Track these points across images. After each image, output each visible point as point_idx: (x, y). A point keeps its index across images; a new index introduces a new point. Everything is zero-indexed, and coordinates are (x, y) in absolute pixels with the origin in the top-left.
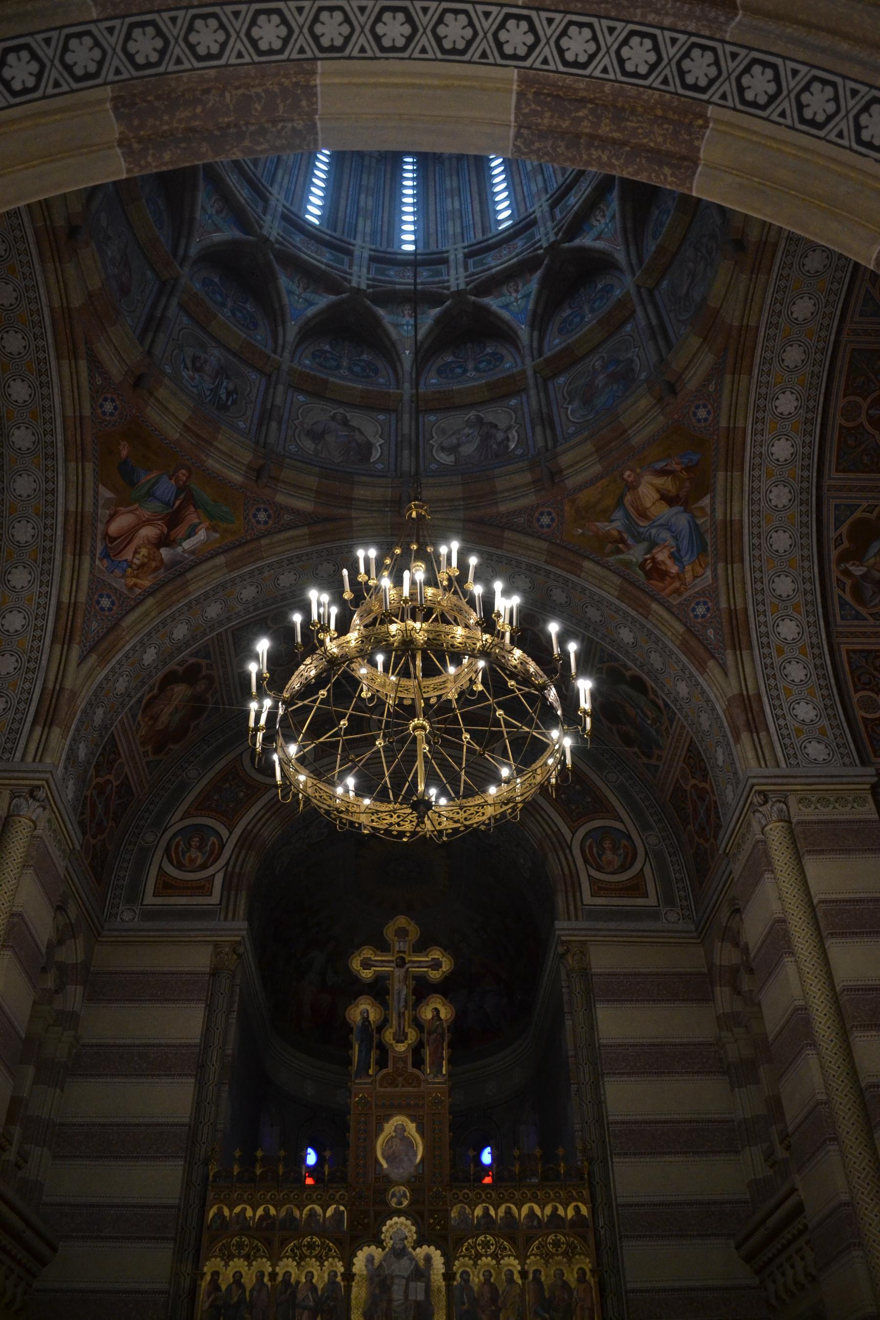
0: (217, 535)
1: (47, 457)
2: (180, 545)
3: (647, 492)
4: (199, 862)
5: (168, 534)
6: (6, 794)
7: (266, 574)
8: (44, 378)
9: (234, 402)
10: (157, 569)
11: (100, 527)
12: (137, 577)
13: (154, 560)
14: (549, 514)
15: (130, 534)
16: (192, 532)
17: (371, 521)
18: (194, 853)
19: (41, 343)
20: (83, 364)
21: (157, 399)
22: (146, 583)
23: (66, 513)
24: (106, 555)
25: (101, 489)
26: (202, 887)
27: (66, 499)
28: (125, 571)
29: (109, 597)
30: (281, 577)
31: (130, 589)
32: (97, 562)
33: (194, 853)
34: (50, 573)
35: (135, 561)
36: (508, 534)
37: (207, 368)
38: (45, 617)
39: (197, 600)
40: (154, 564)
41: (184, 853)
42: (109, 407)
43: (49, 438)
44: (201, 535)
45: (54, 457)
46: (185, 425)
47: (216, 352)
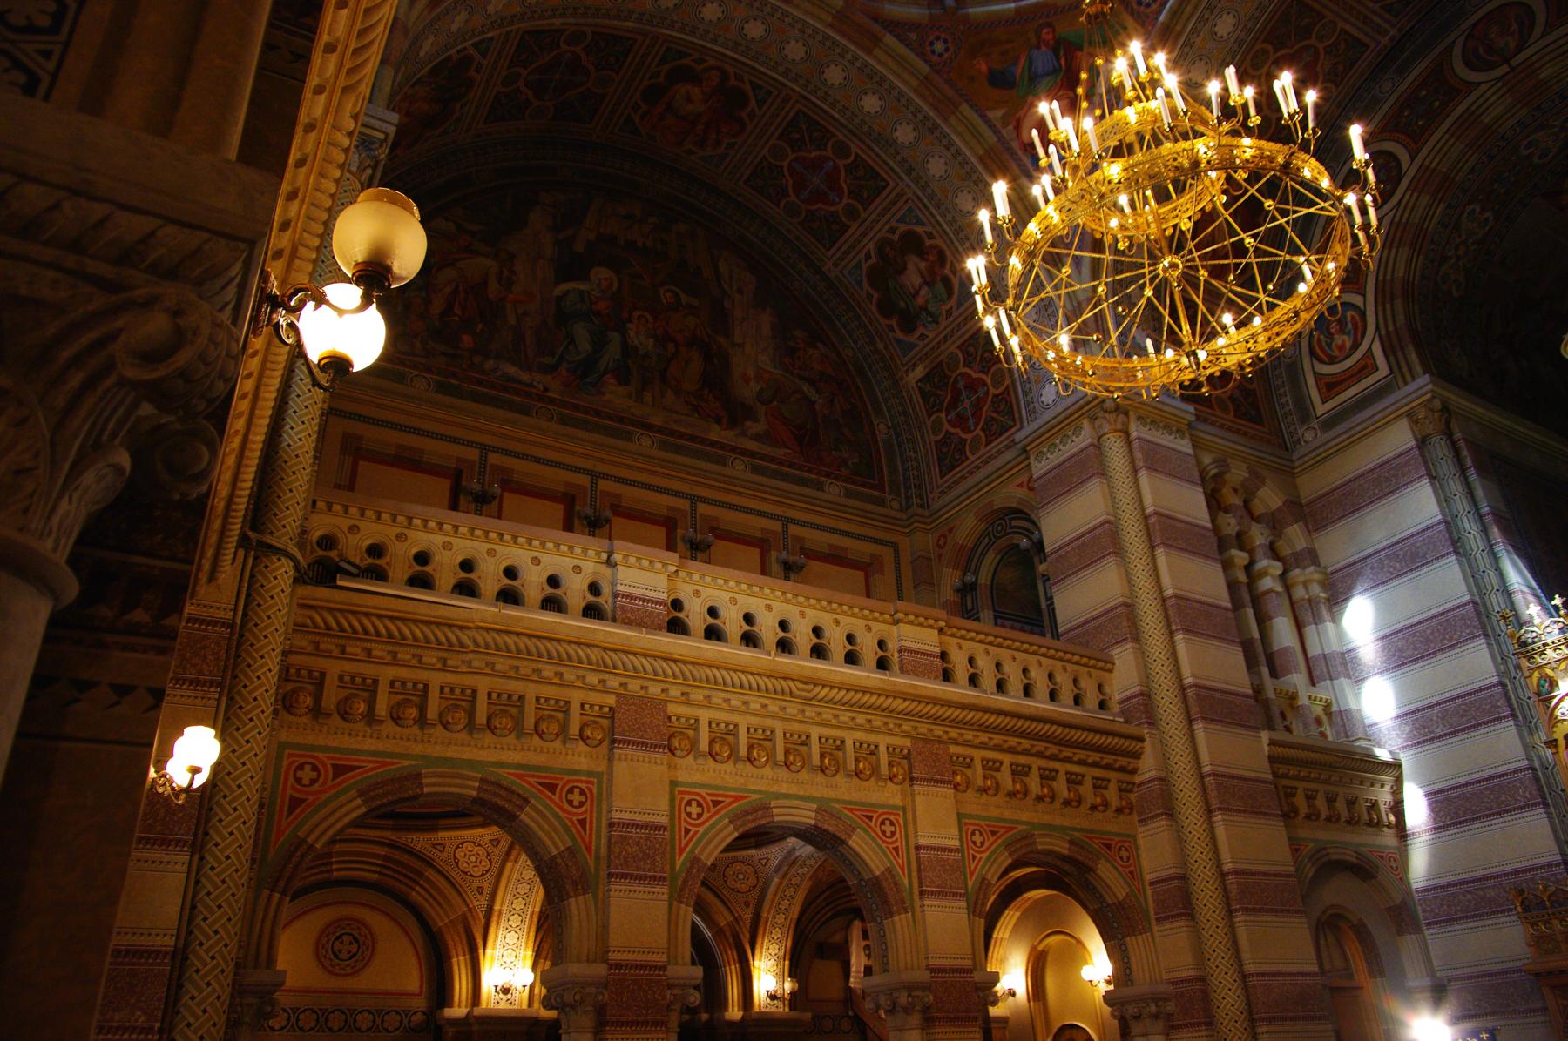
1: (931, 130)
4: (1348, 344)
6: (1086, 423)
7: (1198, 41)
8: (876, 78)
11: (1015, 145)
18: (1339, 339)
19: (849, 56)
20: (889, 39)
23: (981, 159)
25: (991, 115)
26: (1365, 367)
27: (971, 148)
33: (1339, 339)
41: (1329, 346)
42: (939, 47)
43: (920, 116)
45: (936, 127)
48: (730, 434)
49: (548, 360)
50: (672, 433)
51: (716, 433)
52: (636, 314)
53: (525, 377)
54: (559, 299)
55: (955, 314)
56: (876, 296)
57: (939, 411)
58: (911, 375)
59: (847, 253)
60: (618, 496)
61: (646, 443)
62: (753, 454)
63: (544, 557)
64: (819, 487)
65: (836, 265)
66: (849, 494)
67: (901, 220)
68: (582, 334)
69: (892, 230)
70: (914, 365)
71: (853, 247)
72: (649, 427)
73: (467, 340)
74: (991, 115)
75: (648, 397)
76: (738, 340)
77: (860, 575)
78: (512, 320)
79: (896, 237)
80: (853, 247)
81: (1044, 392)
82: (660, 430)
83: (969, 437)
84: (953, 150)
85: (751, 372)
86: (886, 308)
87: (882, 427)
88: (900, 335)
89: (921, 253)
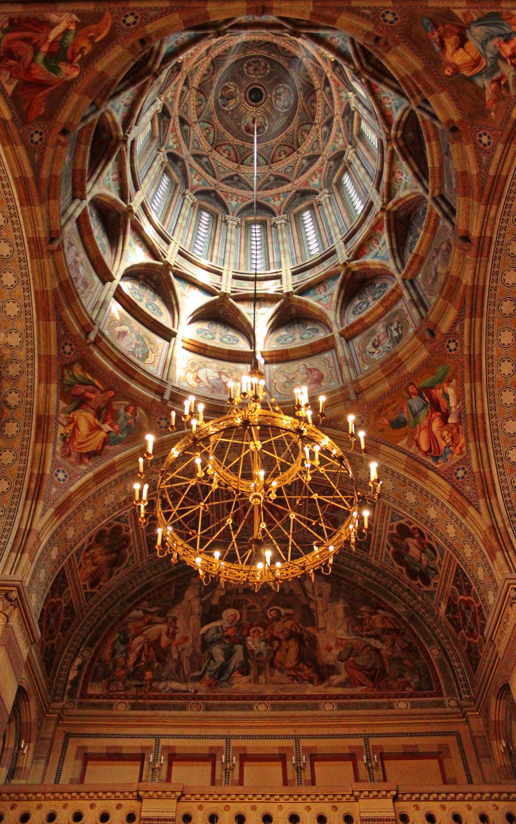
0: (454, 380)
2: (451, 408)
3: (460, 58)
5: (442, 412)
7: (495, 353)
9: (401, 328)
10: (458, 430)
11: (420, 455)
12: (457, 445)
13: (452, 429)
14: (480, 136)
15: (432, 438)
16: (446, 396)
17: (471, 272)
21: (366, 389)
22: (463, 441)
24: (436, 459)
25: (400, 444)
28: (450, 451)
29: (458, 469)
30: (502, 342)
31: (461, 453)
32: (437, 466)
34: (433, 496)
35: (448, 441)
36: (492, 172)
37: (381, 337)
38: (453, 514)
39: (490, 409)
40: (455, 431)
44: (450, 391)
46: (386, 376)
47: (380, 325)
48: (321, 687)
49: (197, 673)
50: (280, 698)
51: (310, 690)
52: (252, 630)
53: (183, 687)
54: (203, 635)
55: (443, 564)
56: (404, 569)
57: (461, 629)
58: (441, 611)
59: (378, 550)
60: (244, 748)
61: (262, 709)
62: (337, 697)
63: (99, 803)
64: (391, 707)
65: (377, 559)
66: (414, 705)
67: (392, 521)
68: (217, 651)
69: (391, 528)
70: (440, 605)
71: (378, 545)
72: (263, 698)
73: (149, 675)
74: (400, 444)
75: (262, 678)
76: (321, 626)
77: (434, 763)
78: (175, 656)
79: (395, 531)
80: (378, 545)
81: (489, 597)
82: (272, 698)
83: (476, 641)
84: (389, 471)
85: (332, 644)
86: (413, 574)
87: (435, 652)
88: (426, 588)
89: (411, 535)
